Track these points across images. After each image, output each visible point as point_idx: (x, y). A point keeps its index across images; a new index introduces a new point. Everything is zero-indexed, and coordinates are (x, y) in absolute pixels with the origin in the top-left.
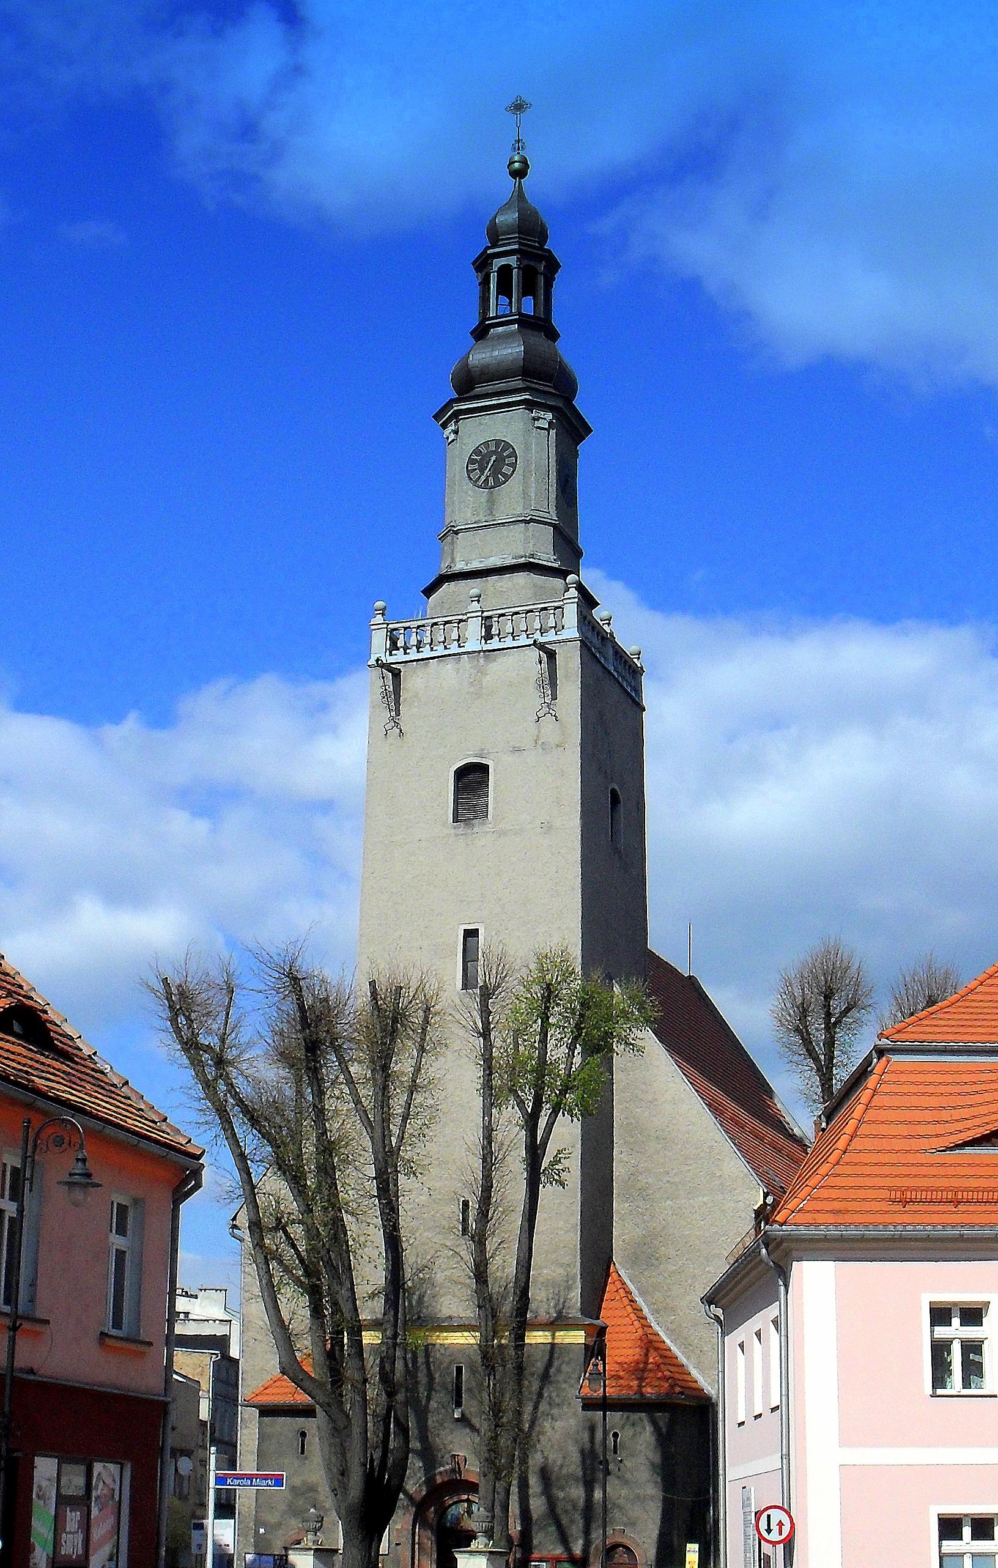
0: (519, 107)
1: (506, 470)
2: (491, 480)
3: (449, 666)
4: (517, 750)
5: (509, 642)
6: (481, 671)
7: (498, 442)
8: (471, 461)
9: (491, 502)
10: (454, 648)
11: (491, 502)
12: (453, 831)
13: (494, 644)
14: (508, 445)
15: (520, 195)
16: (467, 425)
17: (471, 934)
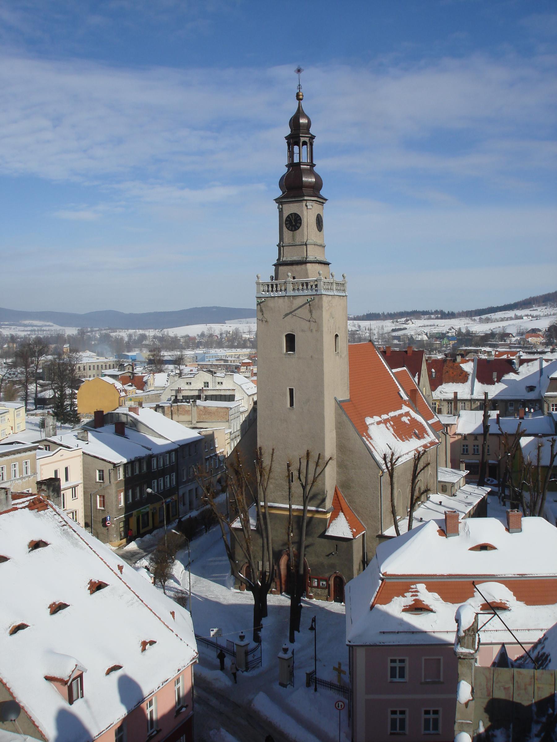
0: (299, 71)
1: (298, 225)
2: (293, 229)
3: (281, 300)
4: (303, 331)
5: (301, 293)
6: (292, 303)
7: (295, 214)
8: (286, 220)
9: (293, 236)
10: (283, 293)
11: (293, 236)
12: (284, 356)
13: (297, 293)
14: (298, 216)
15: (300, 107)
16: (285, 207)
17: (291, 391)
